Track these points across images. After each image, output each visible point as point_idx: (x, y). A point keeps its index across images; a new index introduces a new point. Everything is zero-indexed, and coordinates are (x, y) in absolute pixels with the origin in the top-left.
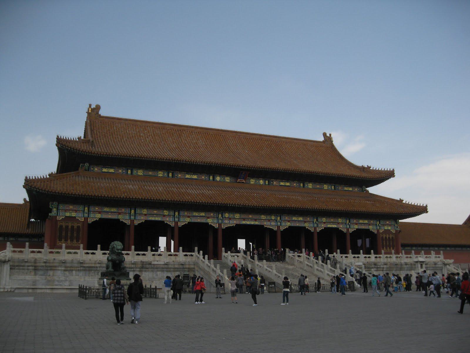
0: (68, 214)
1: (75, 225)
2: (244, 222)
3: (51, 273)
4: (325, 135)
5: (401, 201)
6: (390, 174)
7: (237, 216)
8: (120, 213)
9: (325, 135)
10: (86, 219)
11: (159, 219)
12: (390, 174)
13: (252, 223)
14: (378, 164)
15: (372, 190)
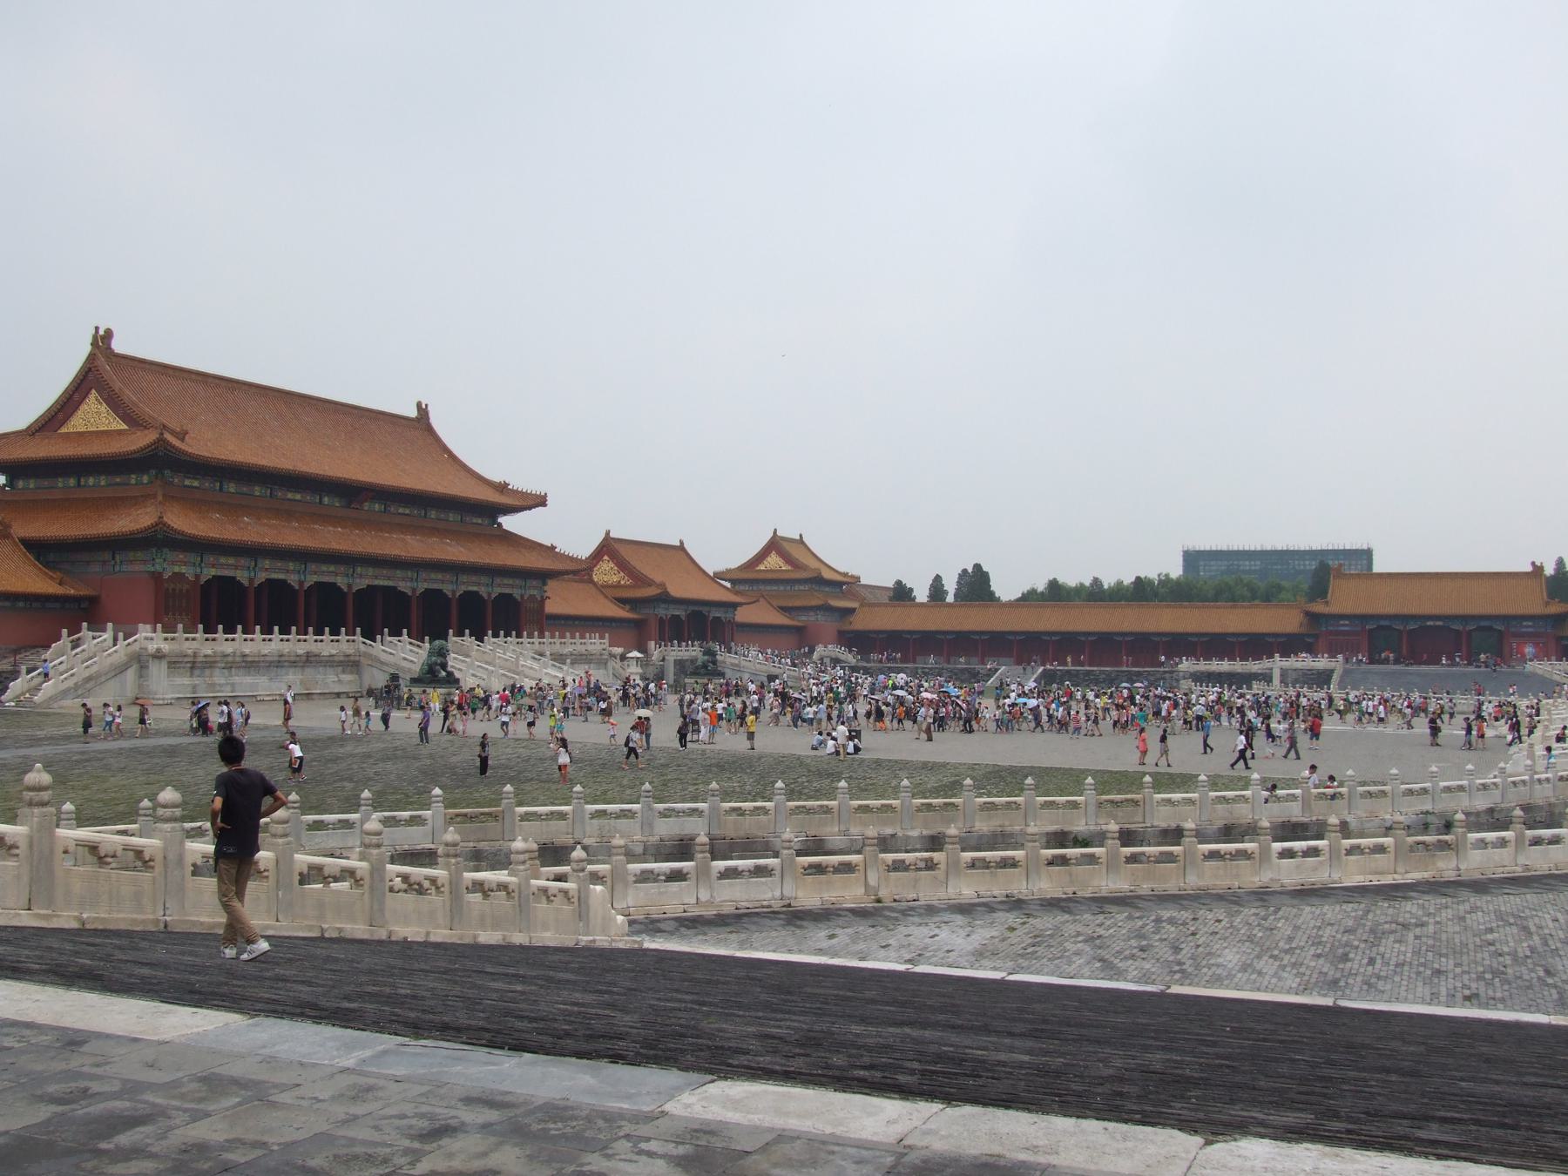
0: (176, 569)
1: (186, 587)
2: (377, 582)
3: (207, 672)
4: (419, 405)
5: (553, 548)
6: (540, 501)
7: (371, 571)
8: (236, 568)
9: (419, 405)
10: (197, 577)
11: (281, 576)
12: (540, 501)
13: (386, 583)
14: (521, 481)
15: (509, 522)
